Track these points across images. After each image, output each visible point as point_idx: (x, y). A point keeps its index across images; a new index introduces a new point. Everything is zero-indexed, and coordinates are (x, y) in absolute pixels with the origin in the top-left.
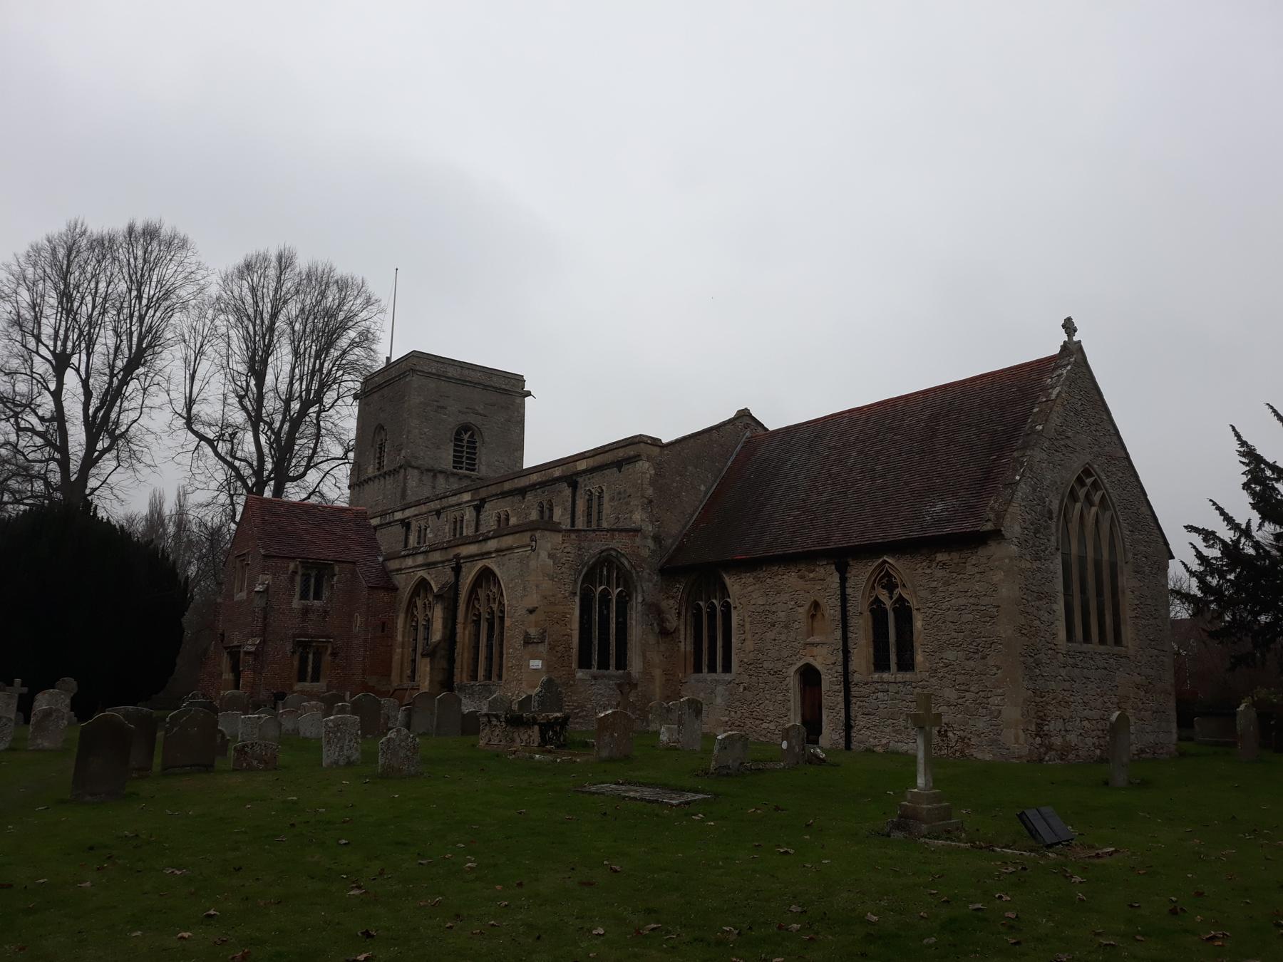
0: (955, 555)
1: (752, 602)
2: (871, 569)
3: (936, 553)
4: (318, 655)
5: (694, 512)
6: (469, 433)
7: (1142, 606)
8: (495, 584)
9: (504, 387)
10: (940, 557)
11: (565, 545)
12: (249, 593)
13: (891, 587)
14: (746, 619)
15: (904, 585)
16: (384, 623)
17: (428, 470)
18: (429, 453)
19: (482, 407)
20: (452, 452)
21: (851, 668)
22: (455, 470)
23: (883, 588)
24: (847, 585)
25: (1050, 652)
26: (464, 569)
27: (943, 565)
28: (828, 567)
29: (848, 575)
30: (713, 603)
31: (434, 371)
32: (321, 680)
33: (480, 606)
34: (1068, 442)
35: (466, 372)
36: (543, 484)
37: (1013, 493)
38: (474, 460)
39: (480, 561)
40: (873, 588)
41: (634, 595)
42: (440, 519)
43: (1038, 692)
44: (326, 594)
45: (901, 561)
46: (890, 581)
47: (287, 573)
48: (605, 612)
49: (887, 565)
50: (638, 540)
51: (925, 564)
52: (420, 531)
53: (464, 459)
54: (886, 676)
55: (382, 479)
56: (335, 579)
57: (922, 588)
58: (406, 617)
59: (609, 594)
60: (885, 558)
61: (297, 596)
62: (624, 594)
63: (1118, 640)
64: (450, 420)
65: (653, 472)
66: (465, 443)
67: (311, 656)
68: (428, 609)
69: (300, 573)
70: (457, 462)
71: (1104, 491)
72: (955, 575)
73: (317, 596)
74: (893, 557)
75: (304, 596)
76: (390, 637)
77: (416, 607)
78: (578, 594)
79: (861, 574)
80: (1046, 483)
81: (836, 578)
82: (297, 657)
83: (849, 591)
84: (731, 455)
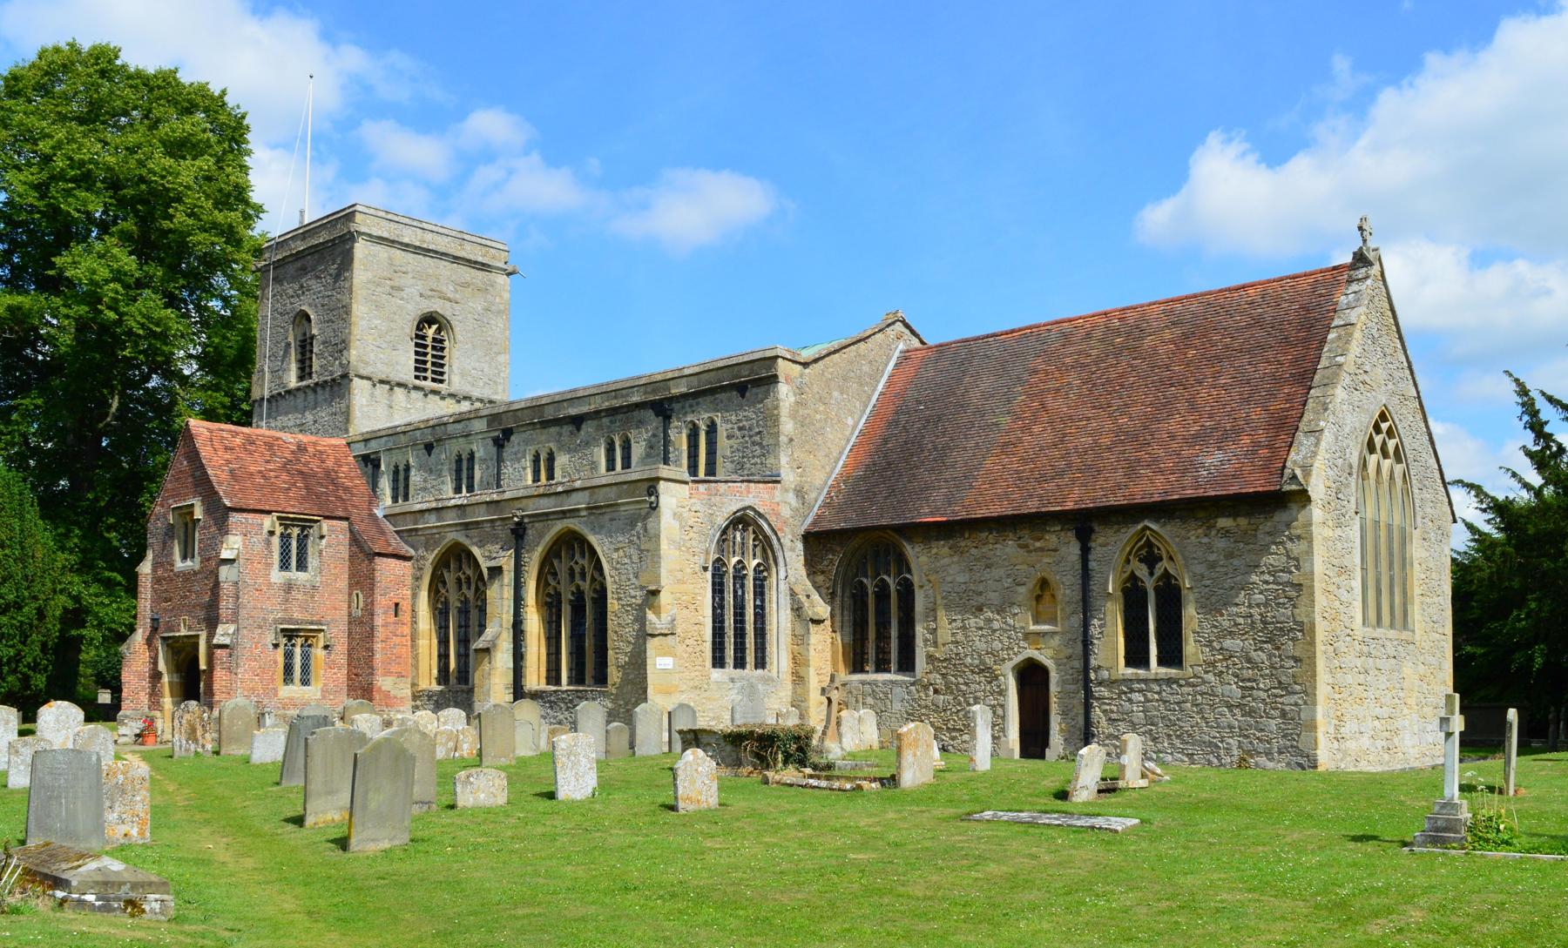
0: (1243, 521)
1: (949, 579)
2: (1129, 535)
3: (1217, 517)
4: (307, 646)
5: (841, 453)
6: (435, 327)
7: (1427, 581)
8: (583, 557)
9: (480, 259)
10: (1224, 522)
11: (693, 501)
12: (205, 560)
13: (1151, 560)
14: (939, 602)
15: (1171, 558)
16: (397, 605)
17: (382, 382)
18: (382, 356)
19: (451, 288)
20: (413, 357)
21: (1093, 662)
22: (417, 382)
23: (1141, 561)
24: (1090, 557)
25: (1348, 638)
26: (530, 532)
27: (1226, 533)
28: (1063, 534)
29: (1092, 544)
30: (883, 580)
31: (385, 235)
32: (312, 681)
33: (559, 583)
34: (1366, 377)
35: (429, 236)
36: (613, 411)
37: (1317, 445)
38: (442, 366)
39: (558, 522)
40: (1128, 561)
41: (774, 570)
42: (432, 456)
43: (1337, 688)
44: (313, 561)
45: (1168, 527)
46: (1151, 552)
47: (261, 534)
48: (740, 593)
49: (1148, 532)
50: (777, 493)
51: (1200, 531)
52: (396, 472)
53: (429, 365)
54: (1141, 672)
55: (309, 392)
56: (324, 541)
57: (1196, 562)
58: (429, 597)
59: (744, 568)
60: (1147, 523)
62: (762, 568)
63: (1405, 626)
64: (409, 306)
65: (792, 399)
66: (429, 342)
67: (298, 650)
68: (464, 587)
69: (278, 533)
70: (420, 367)
71: (1397, 439)
72: (1242, 545)
73: (302, 566)
74: (1157, 521)
75: (285, 565)
77: (444, 583)
78: (710, 568)
79: (1112, 547)
80: (1347, 430)
81: (1074, 550)
82: (281, 650)
83: (1092, 565)
84: (882, 376)
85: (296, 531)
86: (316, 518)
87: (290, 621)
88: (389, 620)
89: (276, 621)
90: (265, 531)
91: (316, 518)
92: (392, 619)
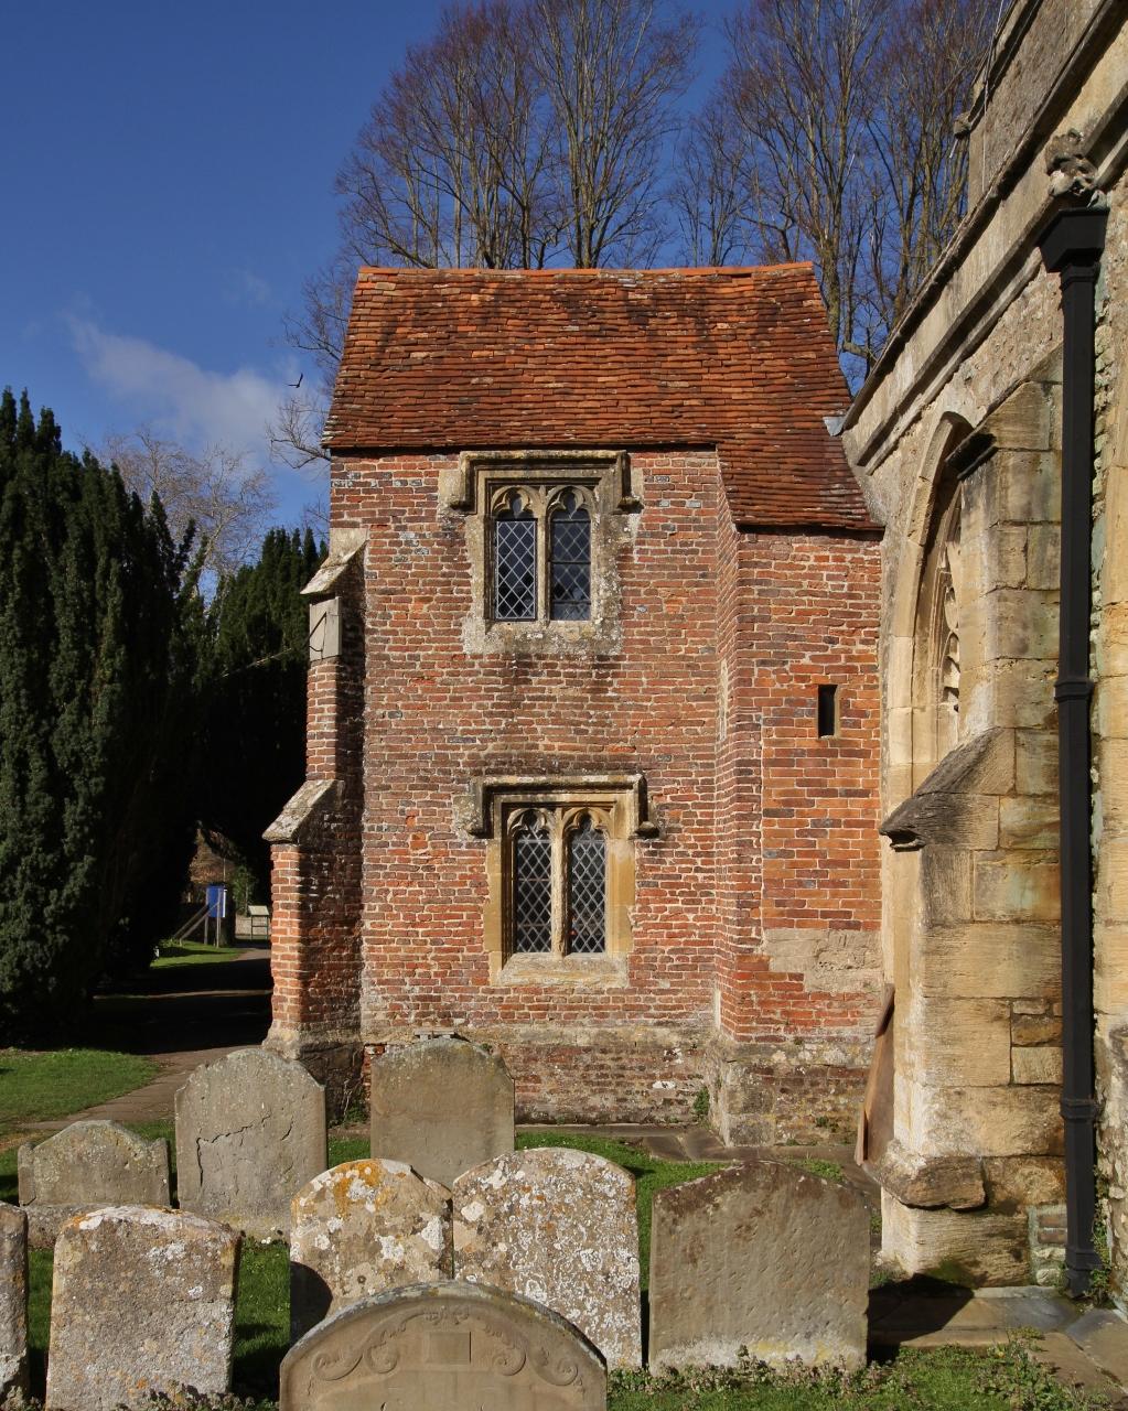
44: (600, 587)
47: (431, 516)
61: (478, 606)
67: (556, 845)
75: (507, 601)
76: (864, 754)
82: (493, 850)
85: (537, 503)
86: (600, 453)
87: (526, 764)
88: (796, 743)
89: (478, 766)
90: (442, 507)
91: (600, 453)
92: (808, 739)
